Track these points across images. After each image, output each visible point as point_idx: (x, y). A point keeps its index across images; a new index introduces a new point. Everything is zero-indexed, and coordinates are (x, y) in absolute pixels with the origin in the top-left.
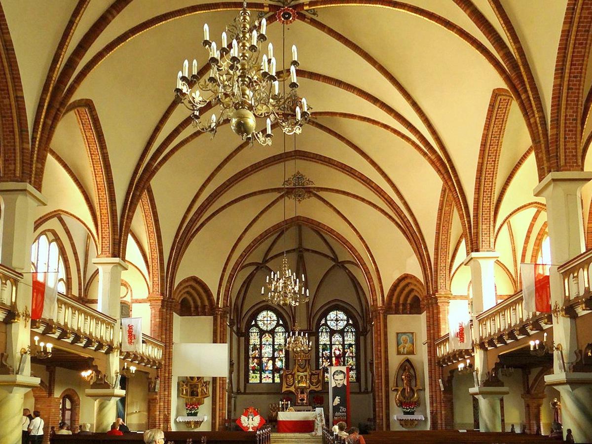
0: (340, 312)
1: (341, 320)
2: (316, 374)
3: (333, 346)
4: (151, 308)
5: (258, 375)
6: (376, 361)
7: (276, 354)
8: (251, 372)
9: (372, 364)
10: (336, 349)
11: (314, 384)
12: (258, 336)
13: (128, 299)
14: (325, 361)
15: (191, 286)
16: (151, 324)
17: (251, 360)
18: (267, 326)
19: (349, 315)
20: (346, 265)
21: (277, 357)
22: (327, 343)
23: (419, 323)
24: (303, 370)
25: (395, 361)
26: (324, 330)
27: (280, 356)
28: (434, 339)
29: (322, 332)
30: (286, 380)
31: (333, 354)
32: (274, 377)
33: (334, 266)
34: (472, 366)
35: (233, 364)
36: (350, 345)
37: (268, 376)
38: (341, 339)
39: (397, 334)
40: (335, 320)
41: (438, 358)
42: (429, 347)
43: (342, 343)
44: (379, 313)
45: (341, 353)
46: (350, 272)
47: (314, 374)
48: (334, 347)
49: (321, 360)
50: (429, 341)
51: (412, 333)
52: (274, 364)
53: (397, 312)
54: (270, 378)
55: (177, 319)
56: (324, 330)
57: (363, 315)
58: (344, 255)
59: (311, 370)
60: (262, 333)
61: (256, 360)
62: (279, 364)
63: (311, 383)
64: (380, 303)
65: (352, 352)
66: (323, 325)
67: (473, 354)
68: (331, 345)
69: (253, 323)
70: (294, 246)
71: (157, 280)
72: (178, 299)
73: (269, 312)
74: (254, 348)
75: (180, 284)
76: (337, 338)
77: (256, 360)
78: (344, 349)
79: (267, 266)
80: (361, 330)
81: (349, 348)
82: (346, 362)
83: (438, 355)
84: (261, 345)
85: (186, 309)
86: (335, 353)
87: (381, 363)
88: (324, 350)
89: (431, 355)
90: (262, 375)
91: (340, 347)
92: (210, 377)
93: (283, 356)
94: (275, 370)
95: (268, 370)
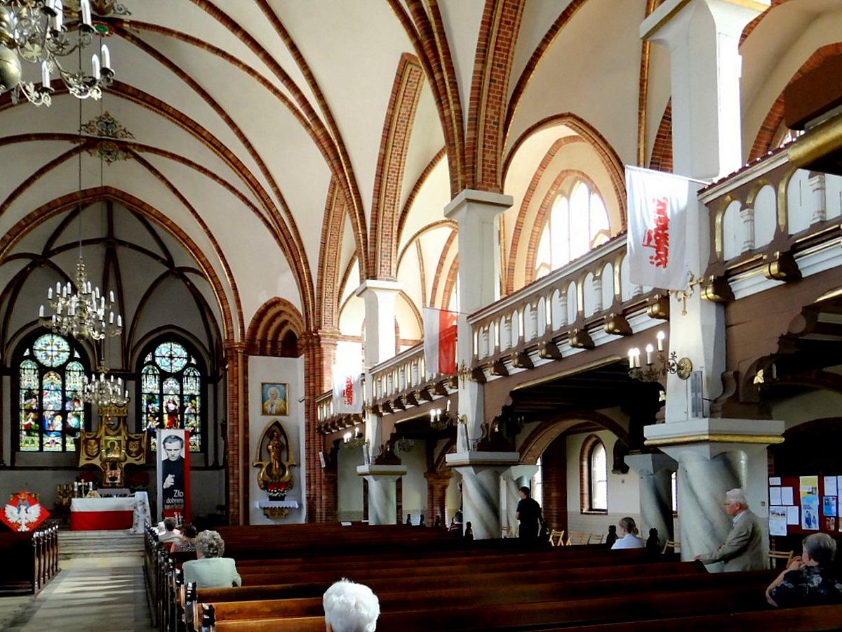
0: (177, 346)
1: (178, 357)
2: (137, 440)
5: (37, 439)
6: (231, 424)
9: (224, 427)
10: (169, 402)
14: (151, 418)
19: (191, 350)
22: (155, 392)
23: (293, 370)
24: (116, 432)
25: (258, 424)
26: (150, 372)
27: (76, 410)
28: (314, 394)
29: (147, 374)
30: (86, 448)
31: (164, 409)
32: (64, 442)
34: (361, 435)
36: (192, 397)
37: (53, 441)
38: (177, 387)
39: (263, 384)
41: (319, 422)
42: (308, 406)
43: (179, 393)
44: (237, 352)
45: (177, 408)
48: (166, 399)
49: (144, 417)
50: (307, 398)
51: (285, 385)
52: (64, 422)
53: (263, 353)
54: (57, 443)
56: (150, 372)
59: (128, 432)
62: (73, 422)
63: (129, 452)
64: (237, 338)
65: (194, 407)
66: (149, 363)
67: (364, 421)
68: (161, 395)
76: (171, 384)
78: (182, 401)
80: (209, 374)
81: (190, 402)
82: (185, 422)
83: (319, 418)
86: (167, 407)
87: (238, 426)
88: (149, 402)
89: (309, 418)
90: (44, 439)
91: (177, 399)
93: (81, 409)
94: (67, 431)
95: (54, 431)
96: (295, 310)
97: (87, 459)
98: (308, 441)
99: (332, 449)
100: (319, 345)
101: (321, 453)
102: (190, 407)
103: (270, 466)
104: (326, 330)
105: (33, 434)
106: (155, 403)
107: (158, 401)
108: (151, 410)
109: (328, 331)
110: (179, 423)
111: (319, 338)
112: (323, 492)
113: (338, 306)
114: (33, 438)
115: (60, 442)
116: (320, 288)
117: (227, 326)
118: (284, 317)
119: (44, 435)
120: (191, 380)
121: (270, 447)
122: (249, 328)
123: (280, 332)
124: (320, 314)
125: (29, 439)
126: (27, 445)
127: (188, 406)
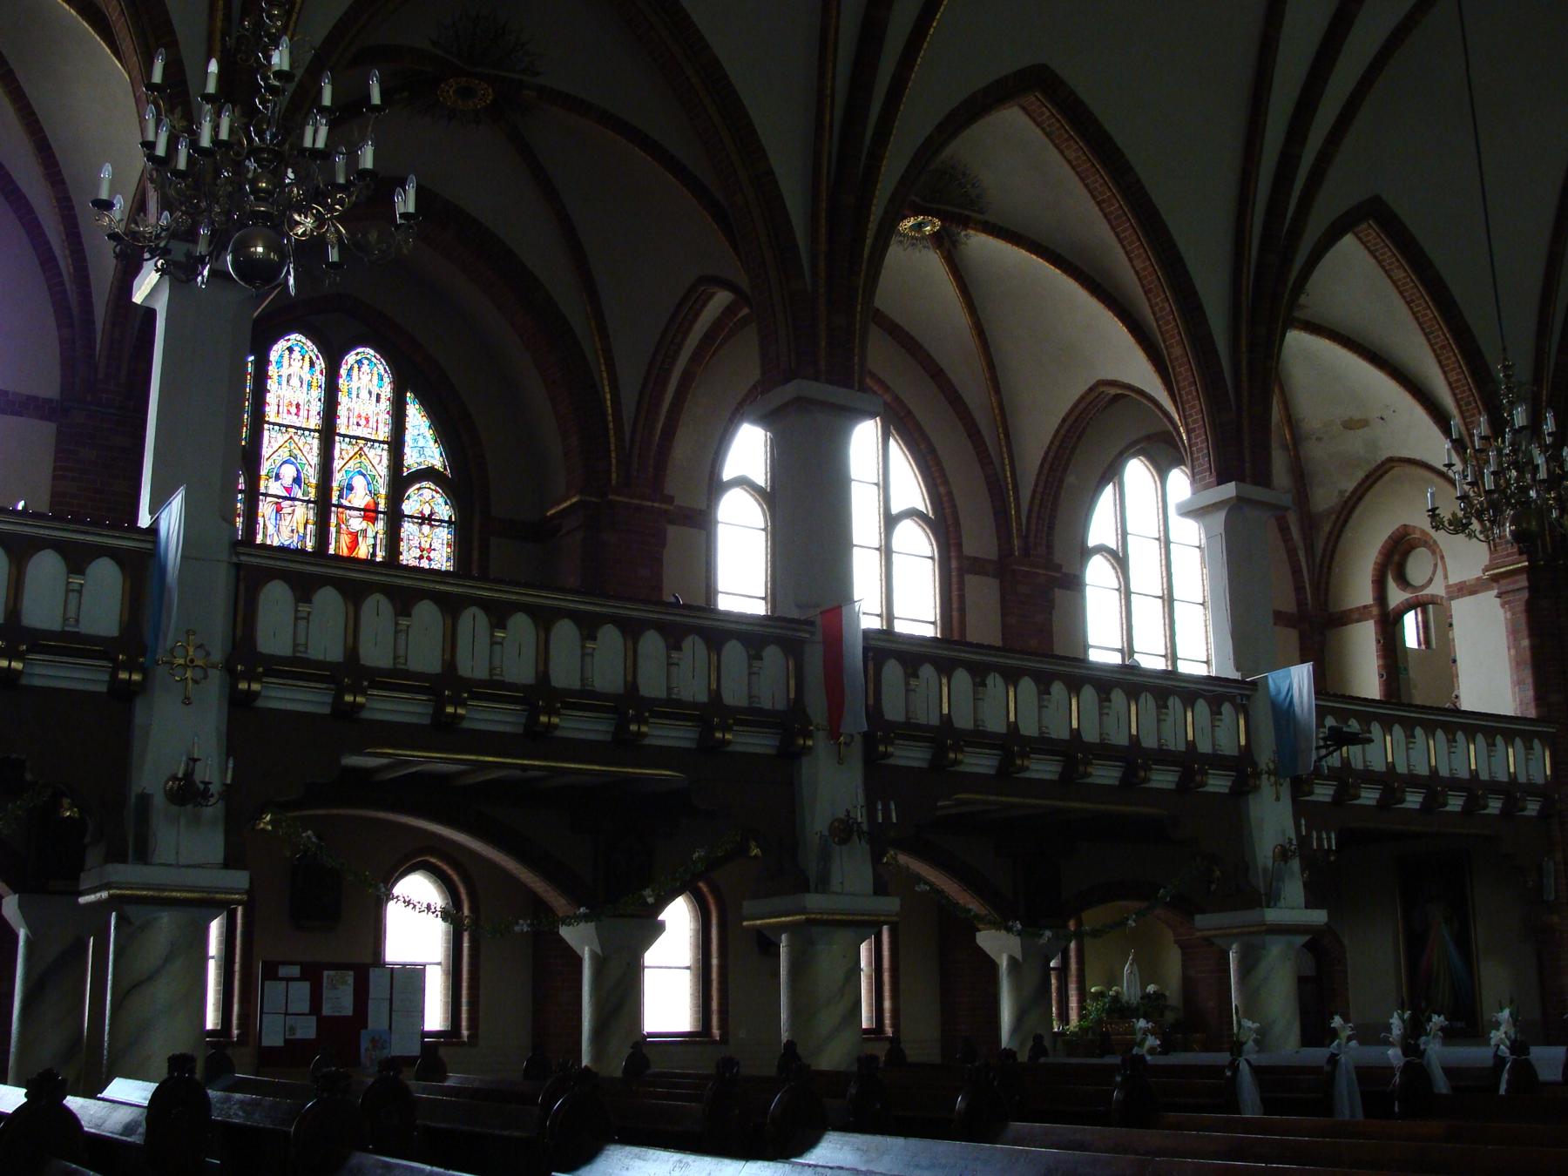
4: (1503, 606)
13: (1437, 589)
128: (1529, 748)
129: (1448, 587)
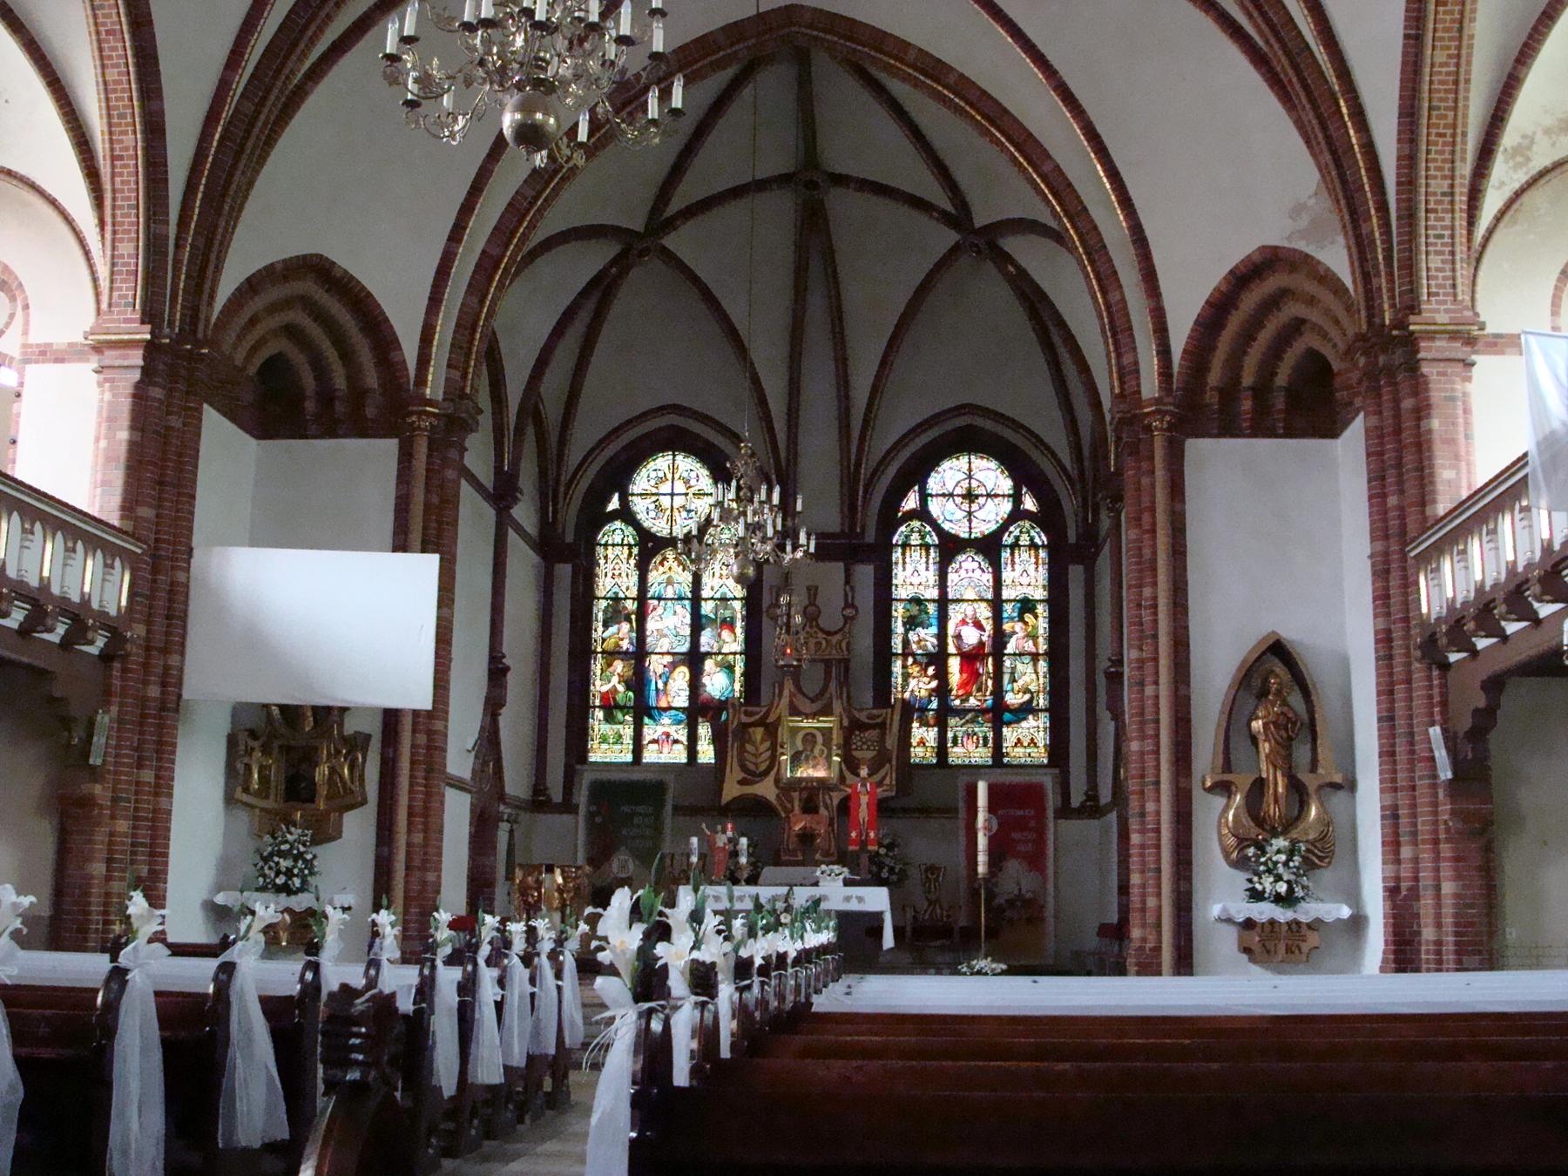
1: (988, 495)
2: (873, 727)
3: (951, 607)
4: (100, 384)
5: (628, 732)
6: (1134, 654)
7: (707, 639)
8: (599, 714)
9: (1115, 678)
10: (964, 622)
11: (864, 772)
12: (632, 562)
14: (915, 670)
15: (307, 303)
16: (97, 448)
17: (597, 666)
18: (671, 520)
20: (1011, 244)
21: (709, 654)
26: (915, 539)
30: (742, 750)
31: (950, 640)
33: (955, 250)
35: (507, 669)
36: (1026, 606)
37: (668, 735)
38: (988, 578)
40: (963, 496)
41: (1424, 623)
43: (989, 596)
44: (1148, 429)
46: (1023, 273)
47: (863, 727)
48: (955, 614)
49: (897, 667)
52: (695, 684)
53: (1229, 429)
54: (676, 741)
55: (219, 435)
57: (1082, 472)
58: (1000, 193)
60: (649, 547)
61: (619, 666)
62: (716, 683)
63: (851, 764)
64: (1150, 386)
65: (1033, 637)
66: (911, 515)
68: (943, 602)
69: (614, 504)
70: (776, 160)
71: (131, 250)
72: (239, 358)
73: (679, 458)
74: (615, 614)
75: (252, 286)
76: (969, 574)
77: (619, 666)
79: (664, 248)
81: (1021, 619)
82: (1006, 678)
83: (1424, 610)
84: (642, 598)
85: (277, 410)
86: (958, 637)
88: (912, 623)
89: (1388, 614)
90: (645, 730)
91: (984, 612)
92: (372, 710)
93: (737, 647)
94: (699, 708)
95: (670, 708)
96: (1327, 279)
97: (742, 782)
98: (1386, 692)
99: (1476, 711)
100: (1413, 366)
101: (1435, 732)
102: (1021, 634)
103: (1259, 785)
104: (1435, 312)
105: (620, 716)
106: (925, 626)
107: (934, 622)
108: (914, 647)
109: (1442, 318)
110: (990, 683)
111: (1410, 343)
112: (1446, 869)
113: (1469, 240)
114: (620, 727)
115: (684, 739)
116: (1408, 182)
117: (1119, 356)
118: (1292, 310)
119: (646, 720)
120: (1024, 556)
121: (1257, 725)
122: (1185, 351)
123: (1280, 358)
124: (1410, 267)
125: (607, 729)
126: (604, 746)
127: (1014, 633)
128: (109, 566)
129: (25, 346)
